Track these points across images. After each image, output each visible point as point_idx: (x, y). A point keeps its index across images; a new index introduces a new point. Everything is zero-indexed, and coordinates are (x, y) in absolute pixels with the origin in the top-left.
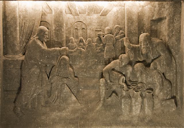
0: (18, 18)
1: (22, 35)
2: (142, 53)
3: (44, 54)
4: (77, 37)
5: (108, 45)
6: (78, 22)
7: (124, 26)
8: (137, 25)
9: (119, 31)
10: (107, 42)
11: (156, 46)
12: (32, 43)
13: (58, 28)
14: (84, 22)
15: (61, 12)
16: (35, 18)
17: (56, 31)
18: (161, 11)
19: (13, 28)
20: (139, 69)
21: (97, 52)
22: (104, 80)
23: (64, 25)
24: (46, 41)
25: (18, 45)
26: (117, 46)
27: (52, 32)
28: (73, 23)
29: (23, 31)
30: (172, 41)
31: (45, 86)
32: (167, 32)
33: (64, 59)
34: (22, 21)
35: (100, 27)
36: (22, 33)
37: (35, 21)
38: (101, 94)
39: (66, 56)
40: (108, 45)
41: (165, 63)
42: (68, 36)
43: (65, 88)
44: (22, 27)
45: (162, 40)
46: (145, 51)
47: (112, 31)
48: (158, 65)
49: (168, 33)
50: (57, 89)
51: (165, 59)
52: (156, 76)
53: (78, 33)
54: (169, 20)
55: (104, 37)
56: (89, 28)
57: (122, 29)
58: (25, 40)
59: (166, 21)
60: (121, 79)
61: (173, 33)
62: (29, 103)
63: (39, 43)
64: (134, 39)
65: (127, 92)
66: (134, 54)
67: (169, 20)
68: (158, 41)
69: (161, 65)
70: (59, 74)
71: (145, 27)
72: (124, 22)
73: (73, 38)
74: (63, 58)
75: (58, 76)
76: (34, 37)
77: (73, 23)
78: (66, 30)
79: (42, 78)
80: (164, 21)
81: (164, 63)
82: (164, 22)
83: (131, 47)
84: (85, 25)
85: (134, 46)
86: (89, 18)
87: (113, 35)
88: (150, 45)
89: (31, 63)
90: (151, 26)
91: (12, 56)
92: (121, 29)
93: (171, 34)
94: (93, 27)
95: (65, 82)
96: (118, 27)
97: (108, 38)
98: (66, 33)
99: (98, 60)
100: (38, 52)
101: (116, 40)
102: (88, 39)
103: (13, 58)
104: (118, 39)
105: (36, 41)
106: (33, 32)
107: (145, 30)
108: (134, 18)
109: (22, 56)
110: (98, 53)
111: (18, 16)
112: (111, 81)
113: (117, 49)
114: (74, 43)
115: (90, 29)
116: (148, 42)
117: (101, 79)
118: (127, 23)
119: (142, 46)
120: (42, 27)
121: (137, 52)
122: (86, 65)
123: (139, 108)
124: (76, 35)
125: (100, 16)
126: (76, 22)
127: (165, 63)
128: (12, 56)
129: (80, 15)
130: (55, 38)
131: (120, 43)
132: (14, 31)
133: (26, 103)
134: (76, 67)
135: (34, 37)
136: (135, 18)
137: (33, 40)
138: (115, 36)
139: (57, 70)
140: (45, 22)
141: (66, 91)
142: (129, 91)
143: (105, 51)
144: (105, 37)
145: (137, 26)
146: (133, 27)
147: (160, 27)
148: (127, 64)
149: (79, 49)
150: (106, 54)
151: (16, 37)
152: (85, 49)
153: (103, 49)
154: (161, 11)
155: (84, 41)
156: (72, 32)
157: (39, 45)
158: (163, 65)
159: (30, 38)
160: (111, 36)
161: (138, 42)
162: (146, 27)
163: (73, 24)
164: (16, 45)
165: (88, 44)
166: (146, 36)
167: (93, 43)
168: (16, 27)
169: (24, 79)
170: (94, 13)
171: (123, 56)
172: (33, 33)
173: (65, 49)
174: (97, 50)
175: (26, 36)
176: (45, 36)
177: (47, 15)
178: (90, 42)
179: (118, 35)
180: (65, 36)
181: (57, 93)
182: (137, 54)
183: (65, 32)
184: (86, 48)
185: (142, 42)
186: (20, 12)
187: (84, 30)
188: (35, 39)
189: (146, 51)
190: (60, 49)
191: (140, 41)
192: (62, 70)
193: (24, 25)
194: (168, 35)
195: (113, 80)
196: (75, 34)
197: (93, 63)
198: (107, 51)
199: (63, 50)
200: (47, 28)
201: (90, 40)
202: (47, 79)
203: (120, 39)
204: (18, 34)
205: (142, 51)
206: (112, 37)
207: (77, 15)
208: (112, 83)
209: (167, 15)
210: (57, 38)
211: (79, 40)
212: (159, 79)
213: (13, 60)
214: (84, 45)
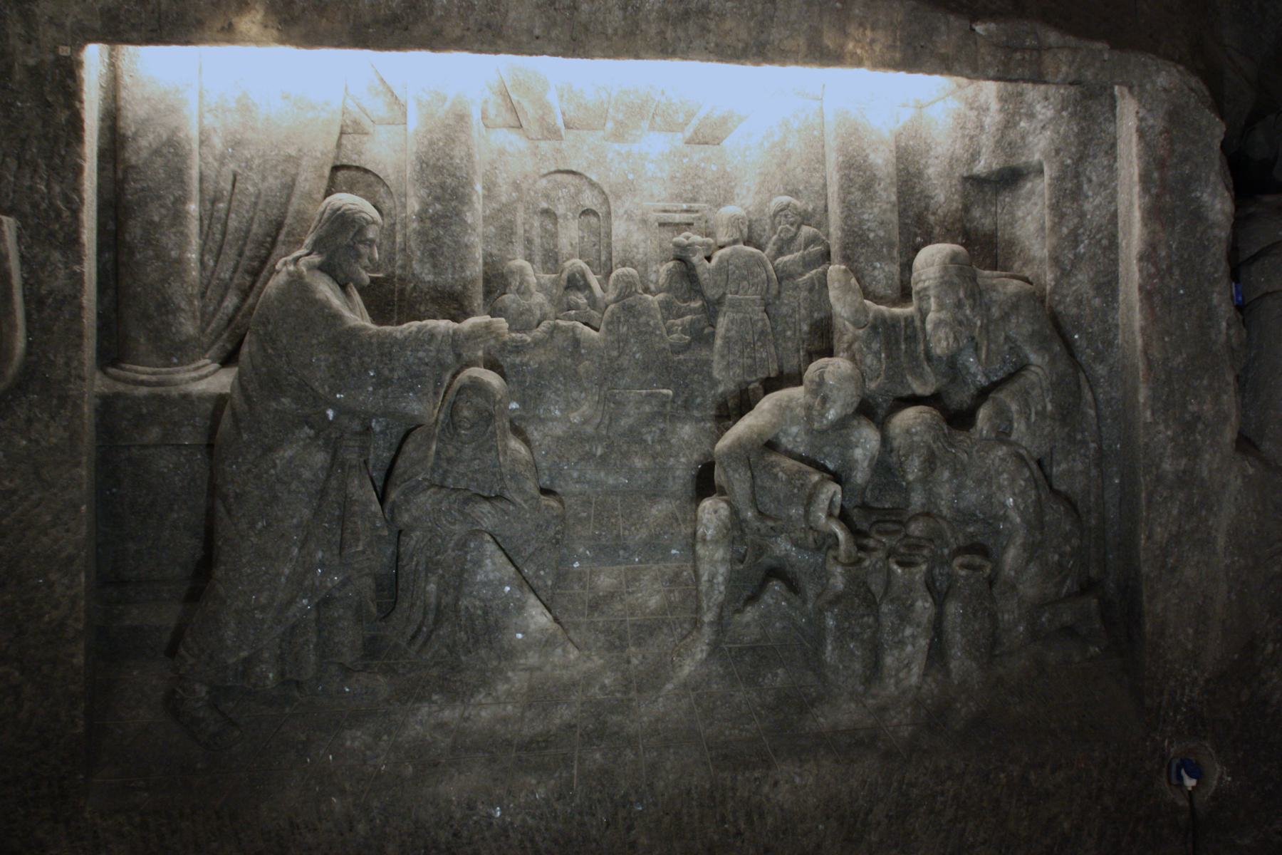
0: (195, 146)
1: (213, 247)
3: (355, 361)
4: (551, 259)
5: (735, 306)
6: (559, 177)
7: (823, 202)
8: (894, 198)
9: (793, 229)
10: (732, 287)
11: (1005, 317)
12: (285, 291)
13: (438, 206)
14: (594, 178)
15: (461, 118)
16: (300, 150)
17: (428, 224)
18: (1012, 135)
19: (162, 206)
20: (916, 438)
21: (671, 345)
22: (723, 505)
23: (479, 187)
24: (368, 281)
25: (191, 303)
26: (784, 310)
27: (398, 227)
28: (526, 176)
29: (225, 225)
30: (1074, 288)
31: (360, 548)
32: (1050, 241)
33: (478, 387)
34: (222, 164)
35: (685, 206)
36: (218, 237)
37: (298, 165)
38: (704, 586)
39: (485, 367)
40: (735, 306)
41: (1049, 407)
42: (495, 251)
43: (488, 562)
44: (214, 201)
45: (1031, 283)
46: (947, 339)
47: (757, 229)
48: (1016, 416)
49: (1054, 248)
50: (432, 566)
51: (1051, 384)
52: (1005, 476)
53: (554, 235)
54: (1059, 180)
55: (709, 259)
56: (621, 211)
57: (813, 222)
58: (238, 275)
59: (1039, 191)
60: (823, 496)
61: (1076, 247)
62: (266, 655)
63: (326, 289)
64: (883, 273)
65: (853, 569)
66: (887, 357)
67: (1058, 179)
68: (1014, 286)
69: (1033, 418)
70: (445, 474)
71: (934, 214)
72: (821, 181)
73: (527, 264)
75: (442, 487)
76: (296, 260)
77: (526, 176)
78: (485, 219)
79: (346, 503)
80: (1029, 185)
81: (1044, 407)
82: (1032, 192)
83: (871, 315)
84: (596, 192)
85: (887, 314)
86: (619, 154)
87: (763, 250)
88: (973, 309)
89: (276, 410)
90: (966, 209)
91: (154, 374)
92: (805, 218)
93: (1071, 256)
94: (646, 204)
95: (487, 523)
96: (788, 205)
97: (737, 267)
98: (486, 239)
99: (676, 395)
100: (320, 343)
101: (780, 280)
102: (613, 275)
103: (160, 384)
104: (791, 276)
105: (307, 280)
106: (284, 231)
107: (932, 228)
108: (880, 161)
109: (215, 371)
110: (678, 349)
111: (194, 134)
112: (760, 512)
113: (784, 331)
114: (532, 294)
115: (630, 218)
116: (961, 294)
117: (707, 504)
118: (841, 187)
119: (931, 317)
120: (344, 200)
121: (903, 347)
122: (607, 422)
124: (542, 246)
125: (688, 142)
126: (545, 176)
127: (1049, 407)
128: (154, 374)
129: (569, 136)
130: (421, 261)
132: (172, 226)
133: (243, 654)
134: (545, 436)
135: (296, 260)
136: (882, 160)
137: (289, 273)
138: (775, 258)
139: (438, 452)
140: (359, 174)
141: (491, 576)
142: (867, 563)
143: (719, 342)
144: (714, 261)
145: (894, 206)
146: (872, 208)
147: (1012, 214)
148: (850, 411)
149: (564, 330)
150: (723, 357)
151: (180, 261)
152: (603, 327)
153: (706, 331)
154: (1012, 135)
155: (594, 280)
156: (522, 232)
157: (324, 306)
158: (1042, 414)
160: (752, 255)
161: (905, 294)
162: (940, 211)
163: (525, 186)
164: (179, 309)
165: (616, 301)
166: (954, 258)
167: (649, 297)
168: (182, 200)
169: (229, 512)
170: (652, 128)
171: (830, 368)
172: (288, 234)
173: (487, 326)
174: (669, 332)
175: (240, 255)
176: (363, 249)
177: (371, 130)
178: (626, 290)
179: (791, 252)
180: (478, 254)
181: (432, 587)
182: (902, 359)
183: (480, 229)
184: (607, 324)
185: (932, 292)
186: (210, 111)
187: (593, 220)
188: (304, 269)
189: (956, 339)
190: (456, 325)
191: (915, 288)
192: (468, 451)
193: (229, 187)
194: (1056, 260)
195: (771, 508)
196: (537, 241)
197: (647, 409)
198: (727, 340)
199: (473, 336)
200: (375, 206)
201: (632, 276)
202: (376, 507)
203: (802, 275)
204: (195, 241)
205: (927, 343)
206: (760, 262)
207: (552, 133)
208: (771, 523)
209: (1047, 157)
210: (435, 266)
211: (565, 276)
212: (1023, 493)
213: (163, 400)
214: (593, 302)
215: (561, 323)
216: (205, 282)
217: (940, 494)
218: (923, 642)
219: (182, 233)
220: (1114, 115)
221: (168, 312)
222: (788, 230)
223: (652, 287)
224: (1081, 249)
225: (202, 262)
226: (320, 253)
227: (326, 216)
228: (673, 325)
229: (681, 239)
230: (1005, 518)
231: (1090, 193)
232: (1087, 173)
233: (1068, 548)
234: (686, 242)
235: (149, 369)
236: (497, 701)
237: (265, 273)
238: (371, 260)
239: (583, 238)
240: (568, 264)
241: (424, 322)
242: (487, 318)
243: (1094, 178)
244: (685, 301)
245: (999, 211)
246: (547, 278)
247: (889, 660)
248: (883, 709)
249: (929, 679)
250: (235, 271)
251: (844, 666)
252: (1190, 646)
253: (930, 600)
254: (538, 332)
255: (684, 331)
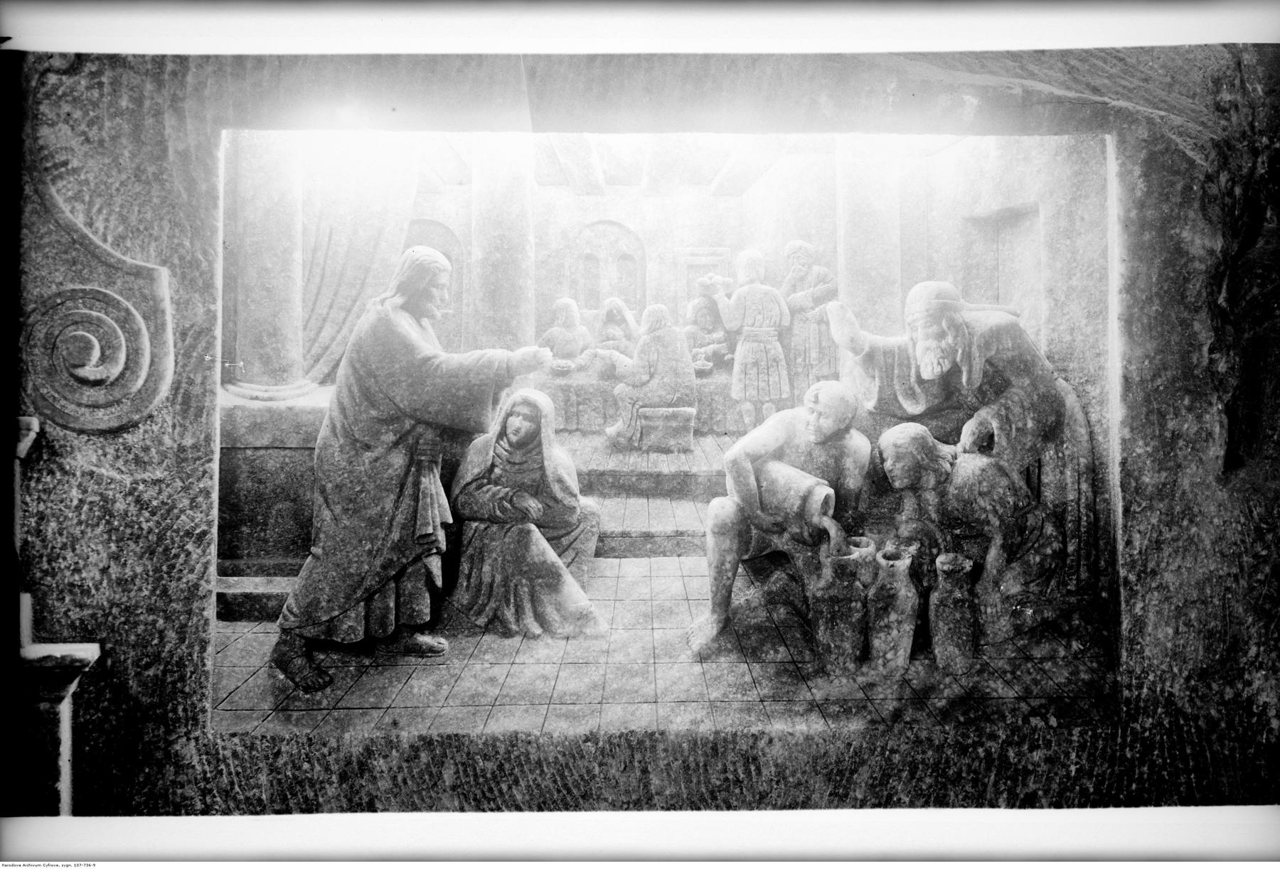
2: (918, 376)
4: (593, 297)
5: (754, 338)
13: (498, 255)
36: (317, 280)
40: (754, 338)
41: (1030, 424)
55: (729, 296)
59: (1041, 226)
61: (1070, 279)
69: (1014, 433)
73: (572, 302)
74: (527, 402)
76: (382, 302)
80: (1028, 223)
99: (699, 412)
102: (646, 312)
103: (271, 399)
104: (802, 310)
110: (701, 374)
123: (906, 644)
128: (266, 391)
131: (814, 326)
135: (382, 302)
143: (737, 367)
144: (734, 297)
152: (635, 355)
153: (726, 358)
155: (629, 316)
159: (355, 301)
175: (335, 295)
176: (434, 290)
178: (657, 325)
179: (803, 289)
180: (531, 294)
184: (643, 352)
188: (389, 308)
189: (939, 363)
190: (510, 354)
193: (327, 239)
200: (445, 254)
203: (813, 309)
204: (299, 283)
211: (604, 312)
214: (628, 337)
215: (600, 351)
216: (307, 316)
217: (927, 500)
218: (908, 628)
219: (289, 277)
220: (1105, 158)
221: (277, 342)
222: (800, 270)
223: (681, 320)
224: (1074, 282)
225: (304, 301)
226: (403, 295)
227: (406, 265)
228: (697, 354)
229: (705, 280)
230: (988, 523)
231: (1083, 231)
232: (1079, 212)
233: (1049, 551)
234: (709, 282)
235: (259, 387)
236: (538, 662)
237: (355, 309)
238: (442, 300)
239: (621, 278)
240: (608, 301)
241: (484, 351)
242: (535, 348)
243: (1086, 217)
244: (710, 332)
245: (1000, 248)
246: (589, 313)
247: (877, 643)
248: (872, 685)
249: (917, 663)
250: (331, 307)
251: (836, 646)
252: (1169, 645)
253: (914, 590)
254: (581, 359)
255: (708, 359)
